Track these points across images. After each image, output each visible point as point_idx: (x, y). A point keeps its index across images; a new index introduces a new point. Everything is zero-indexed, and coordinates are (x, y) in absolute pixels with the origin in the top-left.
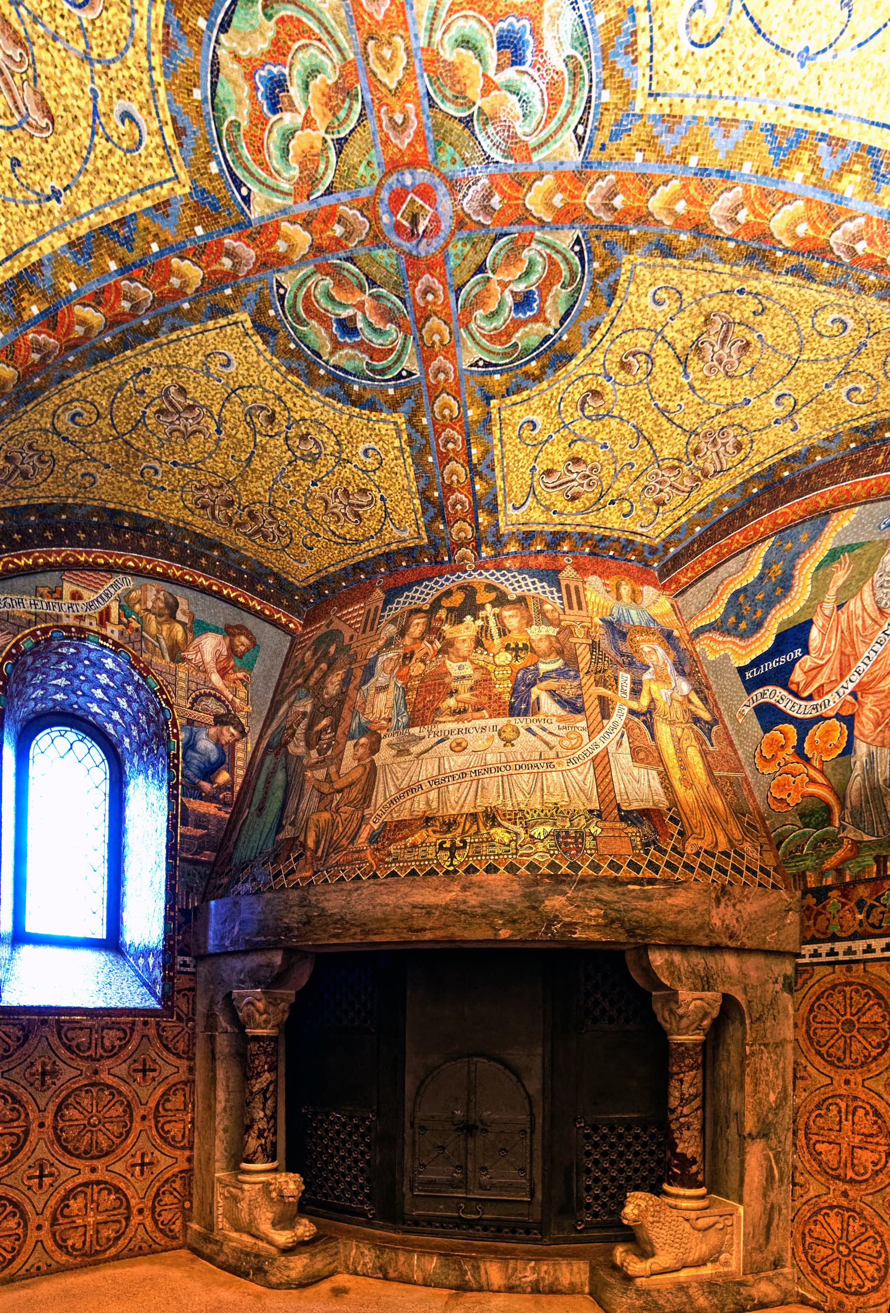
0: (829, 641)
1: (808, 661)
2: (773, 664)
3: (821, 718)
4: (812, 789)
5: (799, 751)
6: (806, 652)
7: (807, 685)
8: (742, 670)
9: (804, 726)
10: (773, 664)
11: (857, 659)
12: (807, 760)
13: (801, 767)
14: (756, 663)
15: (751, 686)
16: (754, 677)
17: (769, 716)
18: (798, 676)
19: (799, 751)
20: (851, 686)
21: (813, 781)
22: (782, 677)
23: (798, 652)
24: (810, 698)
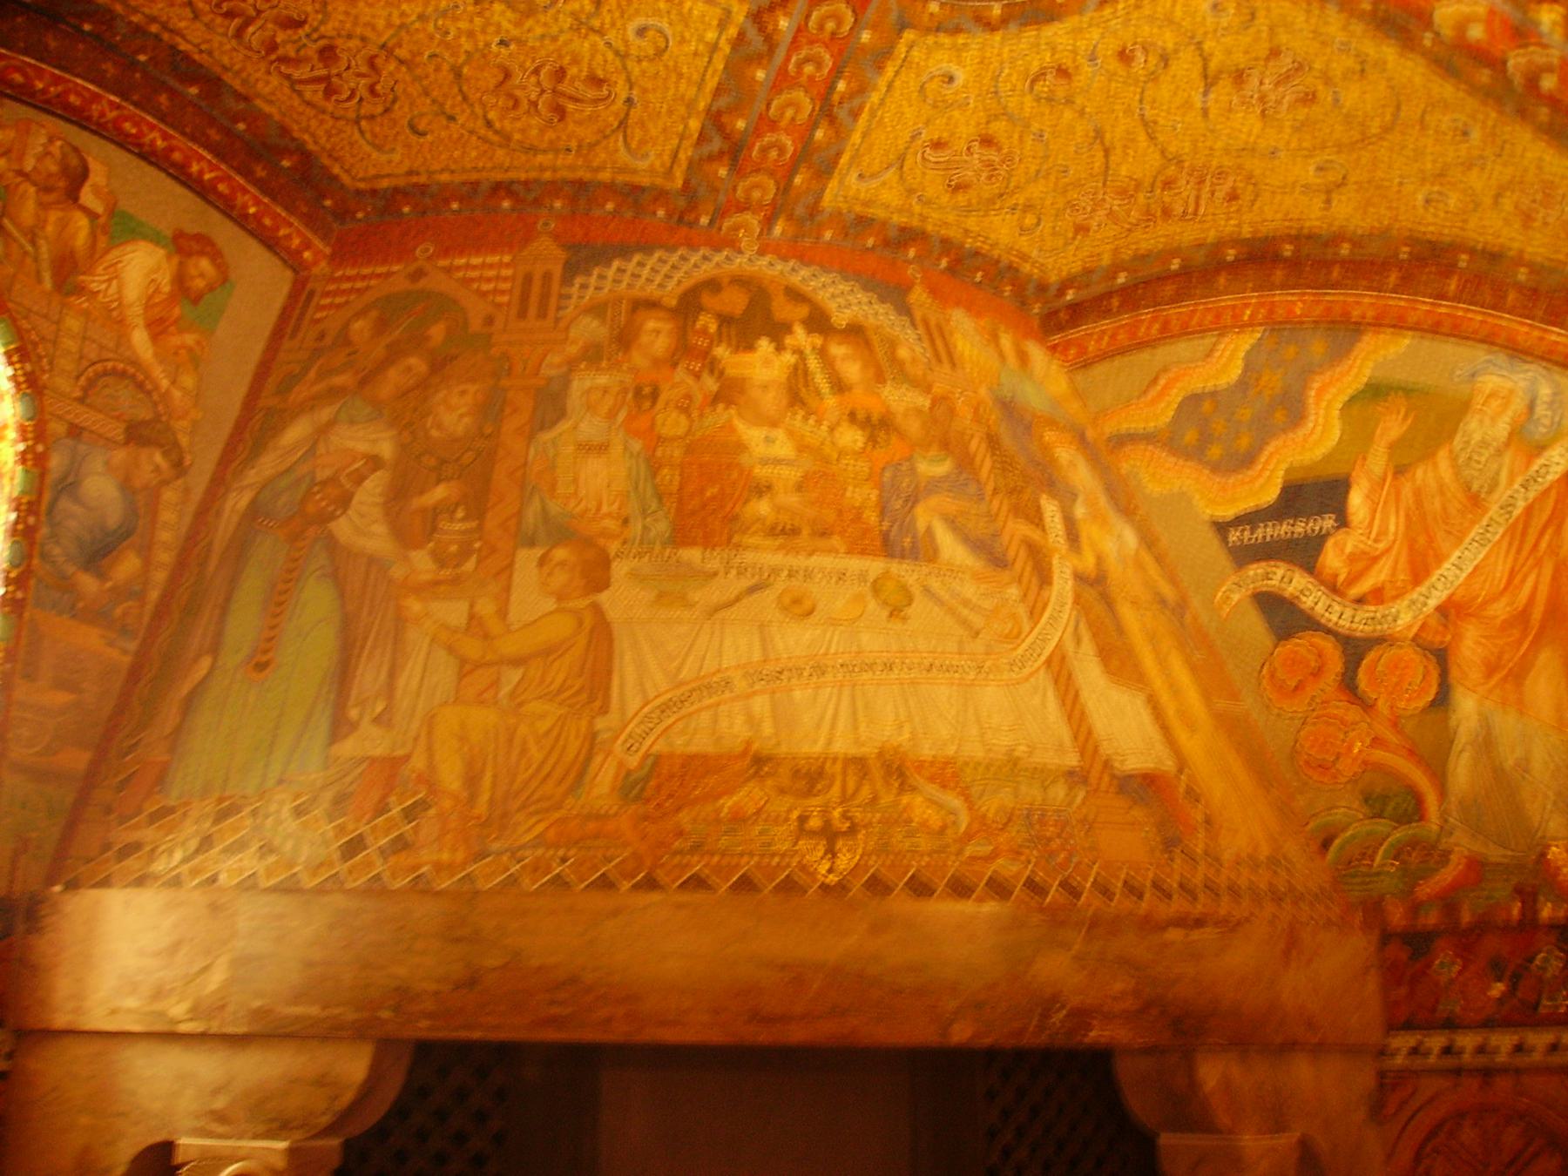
0: (1385, 521)
1: (1351, 541)
2: (1283, 529)
3: (1380, 640)
4: (1379, 755)
5: (1348, 685)
6: (1343, 522)
7: (1353, 579)
8: (1222, 528)
9: (1354, 649)
10: (1283, 529)
11: (1440, 559)
12: (1368, 707)
13: (1353, 714)
14: (1250, 519)
15: (1244, 556)
16: (1244, 540)
17: (1283, 616)
18: (1332, 559)
19: (1348, 685)
20: (1433, 603)
21: (1377, 742)
22: (1305, 554)
23: (1328, 522)
24: (1360, 601)
